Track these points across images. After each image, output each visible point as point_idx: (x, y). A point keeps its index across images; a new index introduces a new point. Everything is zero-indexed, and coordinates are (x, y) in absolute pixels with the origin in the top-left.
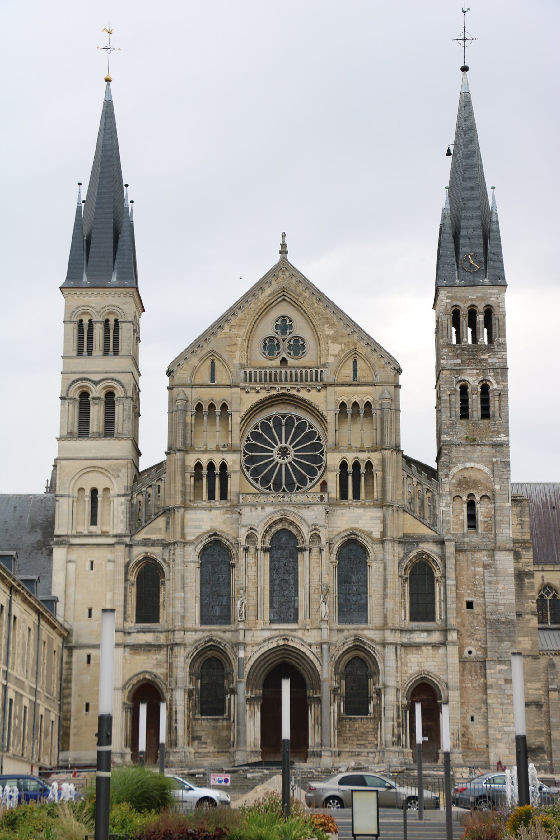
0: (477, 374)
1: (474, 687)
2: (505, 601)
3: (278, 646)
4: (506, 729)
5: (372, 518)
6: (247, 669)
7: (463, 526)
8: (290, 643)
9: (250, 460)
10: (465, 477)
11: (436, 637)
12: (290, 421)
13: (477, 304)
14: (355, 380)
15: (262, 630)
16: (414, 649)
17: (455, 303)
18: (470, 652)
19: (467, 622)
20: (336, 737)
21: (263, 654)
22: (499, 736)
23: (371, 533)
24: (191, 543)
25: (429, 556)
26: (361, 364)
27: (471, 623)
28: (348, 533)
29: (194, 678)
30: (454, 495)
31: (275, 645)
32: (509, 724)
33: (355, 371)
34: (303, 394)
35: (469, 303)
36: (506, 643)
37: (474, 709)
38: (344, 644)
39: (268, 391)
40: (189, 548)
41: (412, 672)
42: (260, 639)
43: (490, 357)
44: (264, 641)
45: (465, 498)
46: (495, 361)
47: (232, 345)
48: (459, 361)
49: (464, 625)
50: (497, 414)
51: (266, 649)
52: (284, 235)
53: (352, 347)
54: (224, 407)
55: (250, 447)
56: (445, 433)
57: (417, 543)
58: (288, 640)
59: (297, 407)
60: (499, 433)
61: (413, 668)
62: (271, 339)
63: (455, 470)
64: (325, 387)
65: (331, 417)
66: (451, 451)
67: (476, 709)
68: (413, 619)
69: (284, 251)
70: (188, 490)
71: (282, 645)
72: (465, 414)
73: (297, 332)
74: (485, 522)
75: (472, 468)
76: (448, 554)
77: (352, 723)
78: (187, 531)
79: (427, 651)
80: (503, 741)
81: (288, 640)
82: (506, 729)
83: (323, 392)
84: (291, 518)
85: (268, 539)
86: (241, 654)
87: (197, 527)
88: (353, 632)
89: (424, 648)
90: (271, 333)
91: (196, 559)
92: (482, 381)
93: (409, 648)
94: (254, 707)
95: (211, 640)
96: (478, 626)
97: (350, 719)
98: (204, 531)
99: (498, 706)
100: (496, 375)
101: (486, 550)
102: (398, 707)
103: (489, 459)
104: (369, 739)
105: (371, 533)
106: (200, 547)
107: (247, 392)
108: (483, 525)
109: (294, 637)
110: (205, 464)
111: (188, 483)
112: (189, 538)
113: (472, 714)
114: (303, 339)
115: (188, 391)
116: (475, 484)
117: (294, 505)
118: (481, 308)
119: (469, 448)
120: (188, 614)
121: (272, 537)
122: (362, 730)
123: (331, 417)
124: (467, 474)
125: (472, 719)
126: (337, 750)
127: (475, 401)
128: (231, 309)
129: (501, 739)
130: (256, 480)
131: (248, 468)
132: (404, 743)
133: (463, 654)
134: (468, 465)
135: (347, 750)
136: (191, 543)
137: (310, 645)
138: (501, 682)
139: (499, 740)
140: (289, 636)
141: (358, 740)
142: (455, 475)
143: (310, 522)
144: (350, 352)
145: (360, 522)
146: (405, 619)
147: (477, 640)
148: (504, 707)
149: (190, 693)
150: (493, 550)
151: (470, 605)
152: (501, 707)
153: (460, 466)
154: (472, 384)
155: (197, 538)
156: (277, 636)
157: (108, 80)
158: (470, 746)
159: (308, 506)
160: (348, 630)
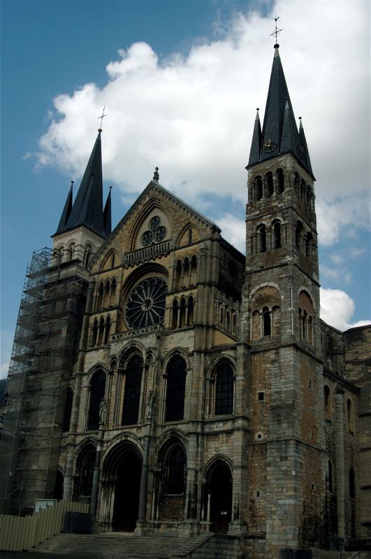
0: (270, 218)
1: (260, 466)
2: (285, 389)
3: (122, 442)
4: (280, 502)
5: (190, 337)
6: (103, 460)
7: (260, 334)
8: (129, 439)
9: (129, 313)
10: (261, 295)
11: (229, 426)
12: (152, 280)
13: (272, 171)
14: (190, 244)
15: (113, 430)
16: (214, 436)
17: (257, 175)
18: (260, 436)
19: (258, 411)
20: (158, 512)
21: (113, 448)
22: (274, 509)
23: (188, 349)
24: (86, 374)
25: (228, 360)
26: (194, 232)
27: (261, 411)
28: (174, 351)
29: (82, 469)
30: (253, 310)
31: (120, 440)
32: (283, 497)
33: (190, 237)
34: (158, 261)
35: (267, 172)
36: (283, 425)
37: (259, 485)
38: (164, 437)
39: (138, 265)
40: (85, 378)
41: (210, 456)
42: (111, 437)
43: (279, 203)
44: (113, 438)
45: (261, 311)
46: (283, 204)
47: (122, 242)
48: (258, 212)
49: (256, 414)
50: (285, 242)
51: (114, 444)
52: (157, 169)
53: (187, 222)
54: (114, 281)
55: (130, 305)
56: (248, 266)
57: (220, 351)
58: (127, 436)
59: (157, 272)
60: (285, 255)
61: (212, 453)
62: (147, 233)
63: (253, 291)
64: (169, 253)
65: (171, 271)
66: (251, 278)
67: (261, 486)
68: (217, 413)
69: (156, 176)
70: (89, 339)
71: (125, 441)
72: (264, 249)
73: (162, 224)
74: (277, 327)
75: (266, 286)
76: (238, 356)
77: (170, 501)
78: (85, 366)
79: (223, 437)
80: (277, 513)
81: (127, 436)
82: (280, 502)
83: (168, 257)
84: (137, 346)
85: (126, 363)
86: (98, 449)
87: (91, 363)
88: (172, 427)
89: (220, 436)
90: (147, 230)
91: (88, 384)
92: (273, 223)
93: (210, 437)
94: (109, 489)
95: (89, 441)
96: (266, 413)
97: (169, 497)
98: (93, 365)
99: (274, 481)
100: (283, 214)
101: (273, 349)
102: (196, 486)
103: (277, 277)
104: (180, 513)
105: (188, 349)
106: (91, 376)
107: (127, 269)
108: (275, 331)
109: (131, 433)
110: (98, 320)
111: (89, 334)
112: (86, 371)
113: (258, 489)
114: (164, 227)
115: (96, 276)
116: (266, 299)
117: (139, 337)
118: (274, 173)
119: (263, 273)
120: (79, 423)
121: (129, 362)
122: (175, 506)
123: (171, 271)
124: (262, 292)
125: (258, 495)
126: (156, 522)
127: (270, 239)
128: (122, 220)
129: (275, 511)
130: (131, 326)
131: (127, 319)
132: (203, 517)
133: (254, 438)
134: (262, 285)
135: (165, 522)
136: (86, 374)
137: (140, 439)
138: (278, 460)
139: (273, 512)
140: (127, 433)
141: (173, 514)
142: (253, 295)
143: (147, 346)
144: (186, 225)
145: (182, 341)
146: (210, 413)
147: (265, 425)
148: (280, 482)
149: (75, 478)
150: (277, 349)
151: (261, 396)
152: (277, 482)
153: (257, 287)
154: (267, 225)
155: (90, 370)
156: (120, 434)
157: (100, 131)
158: (255, 519)
159: (146, 336)
160: (169, 425)
